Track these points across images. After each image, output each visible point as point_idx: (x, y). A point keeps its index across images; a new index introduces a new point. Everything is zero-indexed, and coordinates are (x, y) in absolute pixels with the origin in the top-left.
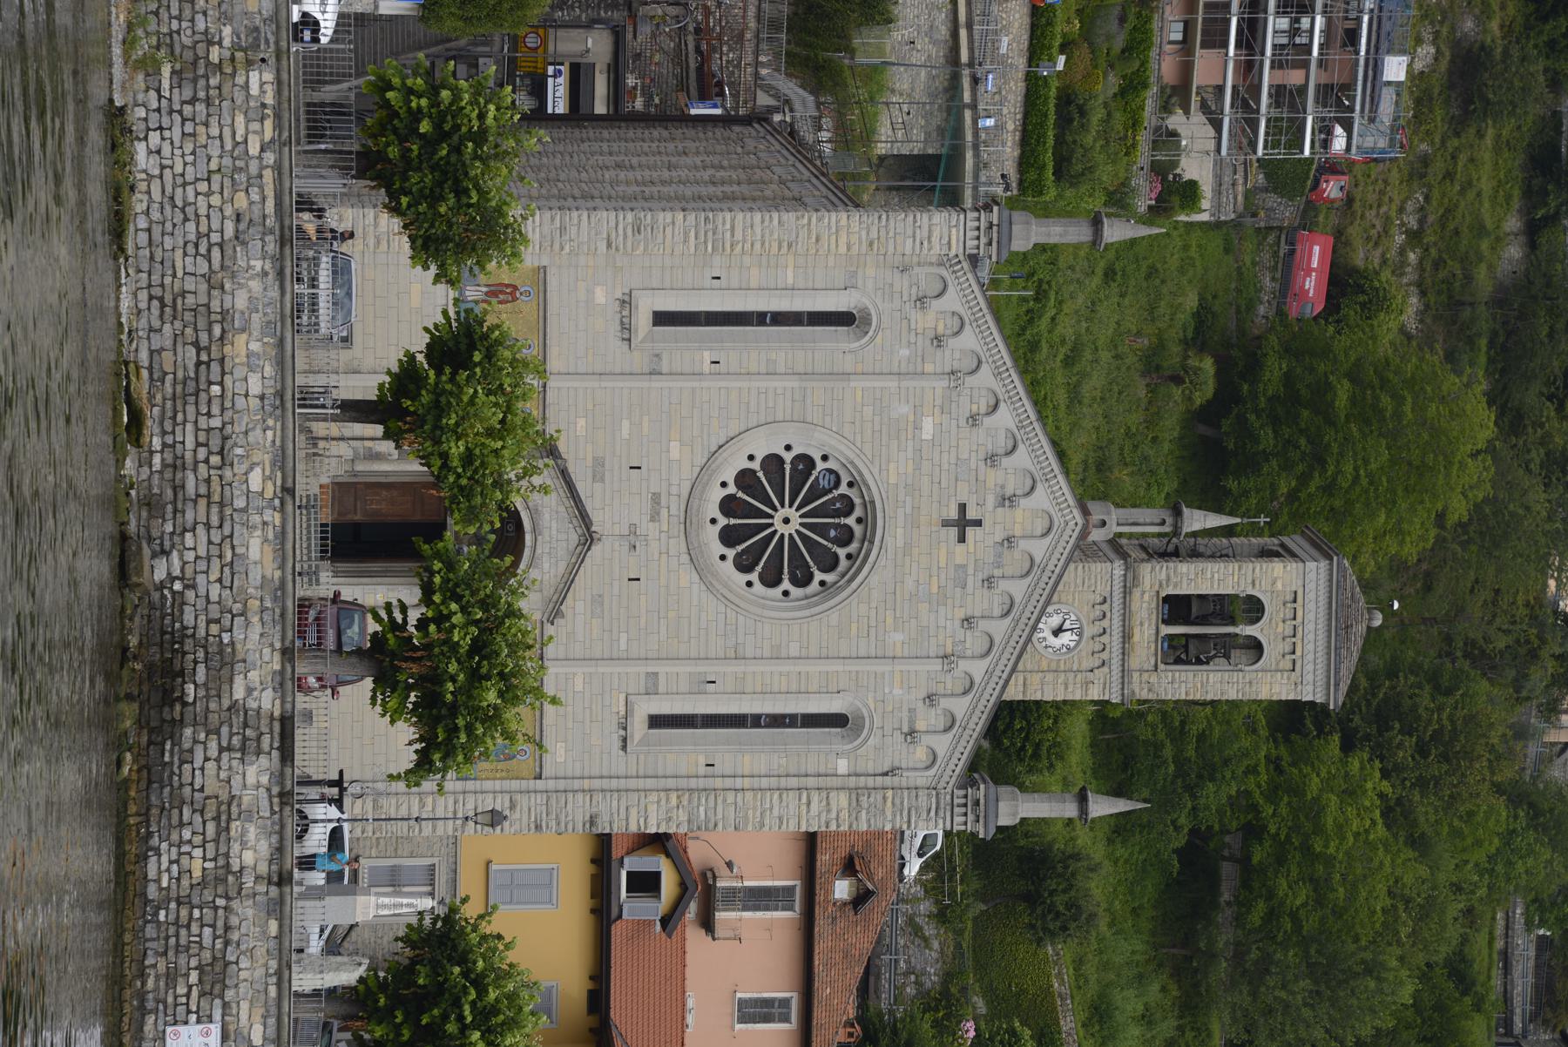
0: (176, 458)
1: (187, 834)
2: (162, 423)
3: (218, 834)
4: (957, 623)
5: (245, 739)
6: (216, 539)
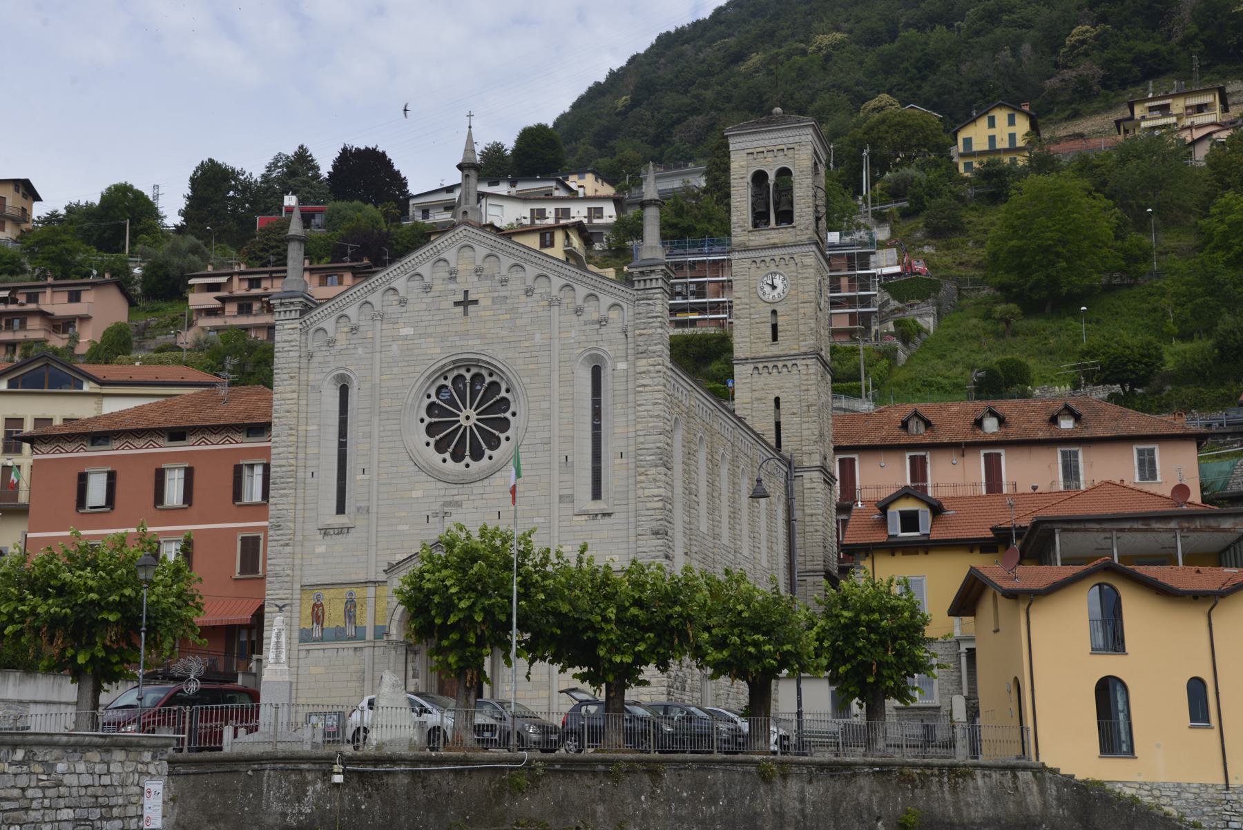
4: (529, 299)
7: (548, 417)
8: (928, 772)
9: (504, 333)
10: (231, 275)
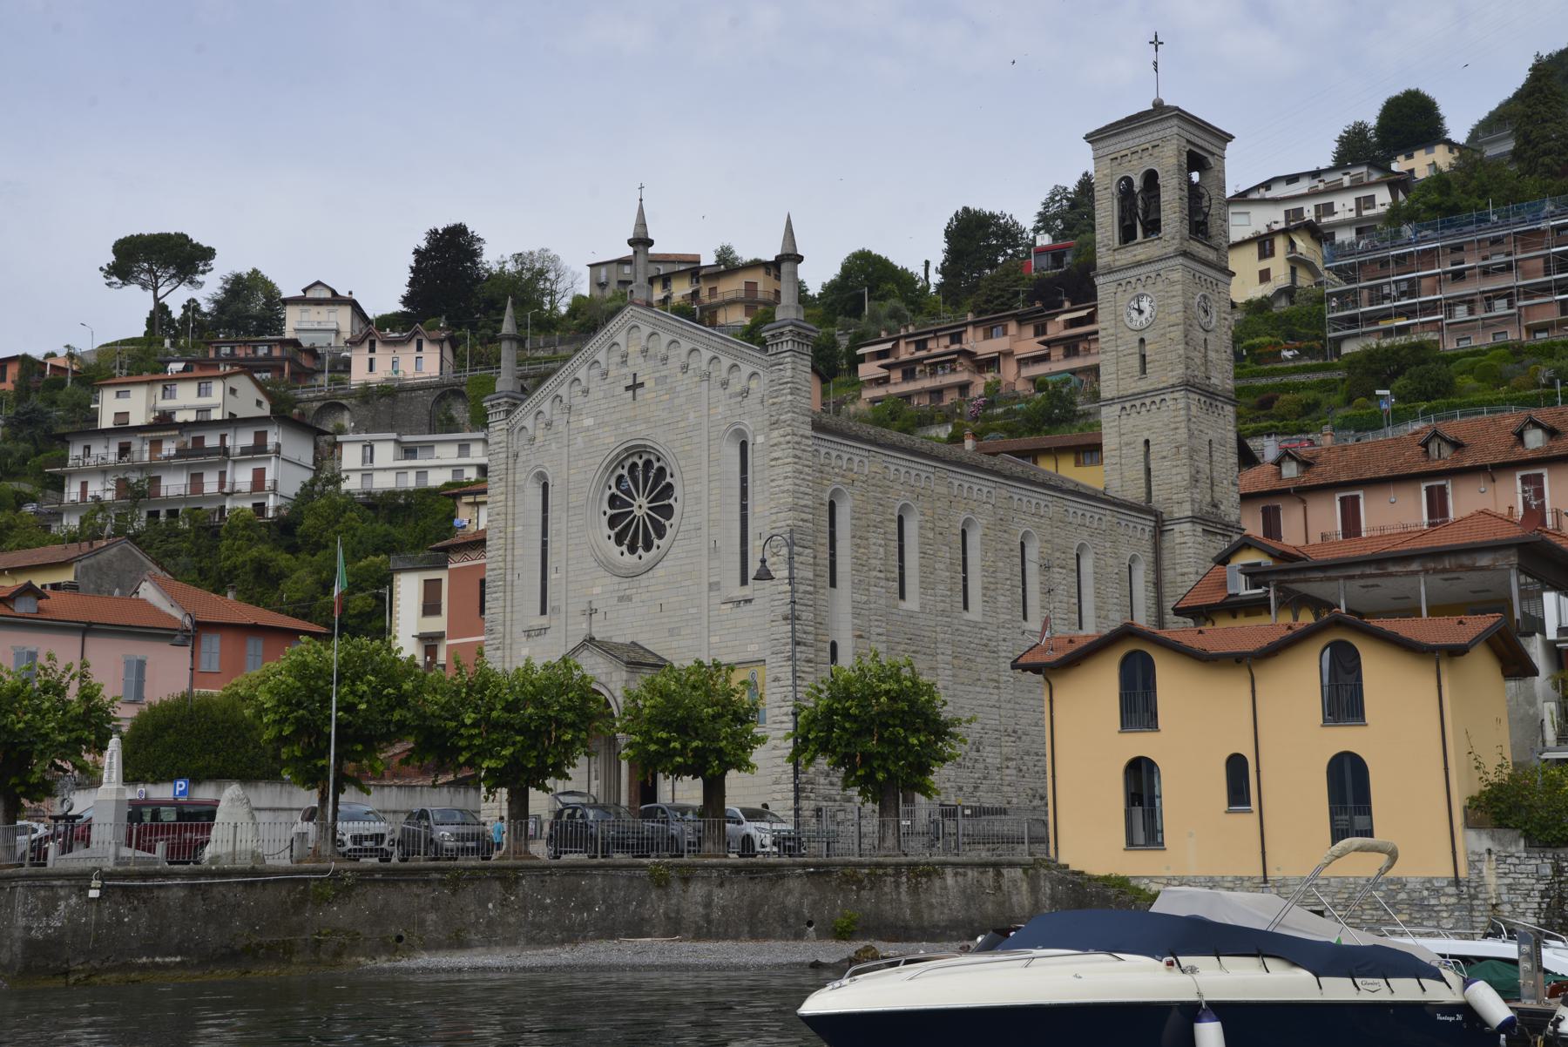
8: (880, 872)
10: (898, 339)
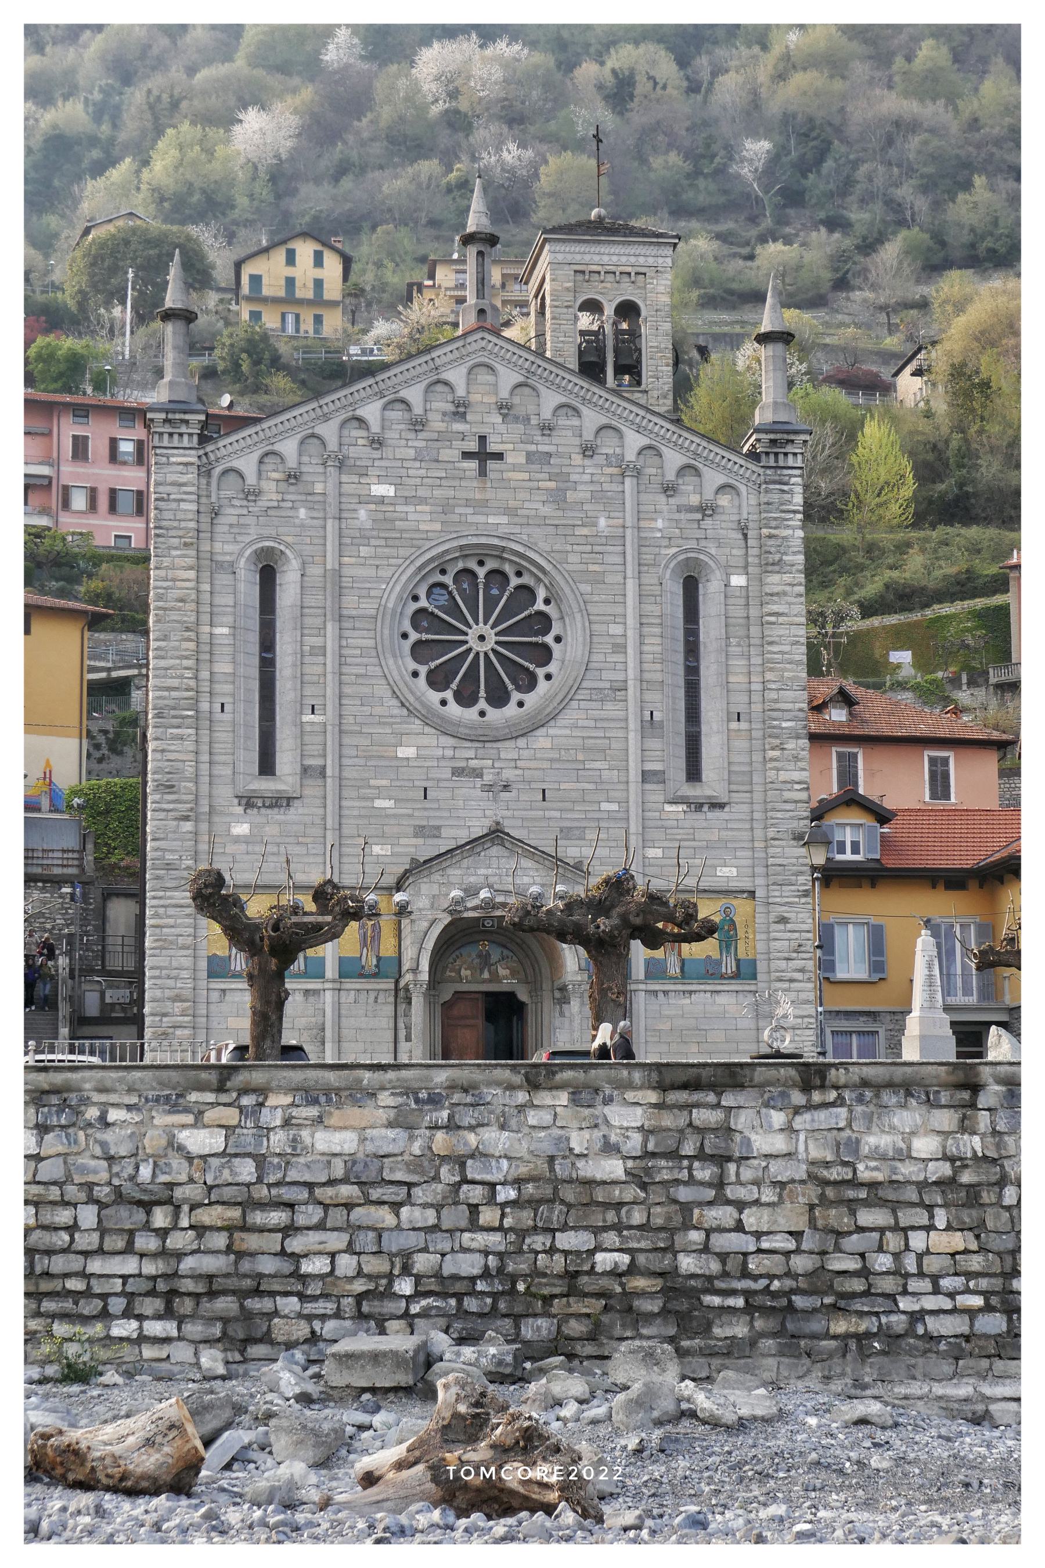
0: (152, 1293)
1: (883, 1262)
2: (85, 1320)
3: (883, 1203)
4: (587, 462)
5: (701, 1156)
6: (315, 1214)
7: (620, 648)
9: (546, 510)
